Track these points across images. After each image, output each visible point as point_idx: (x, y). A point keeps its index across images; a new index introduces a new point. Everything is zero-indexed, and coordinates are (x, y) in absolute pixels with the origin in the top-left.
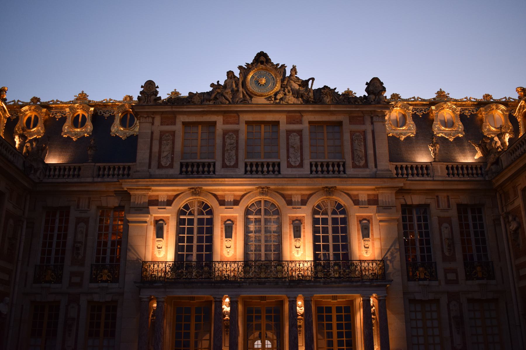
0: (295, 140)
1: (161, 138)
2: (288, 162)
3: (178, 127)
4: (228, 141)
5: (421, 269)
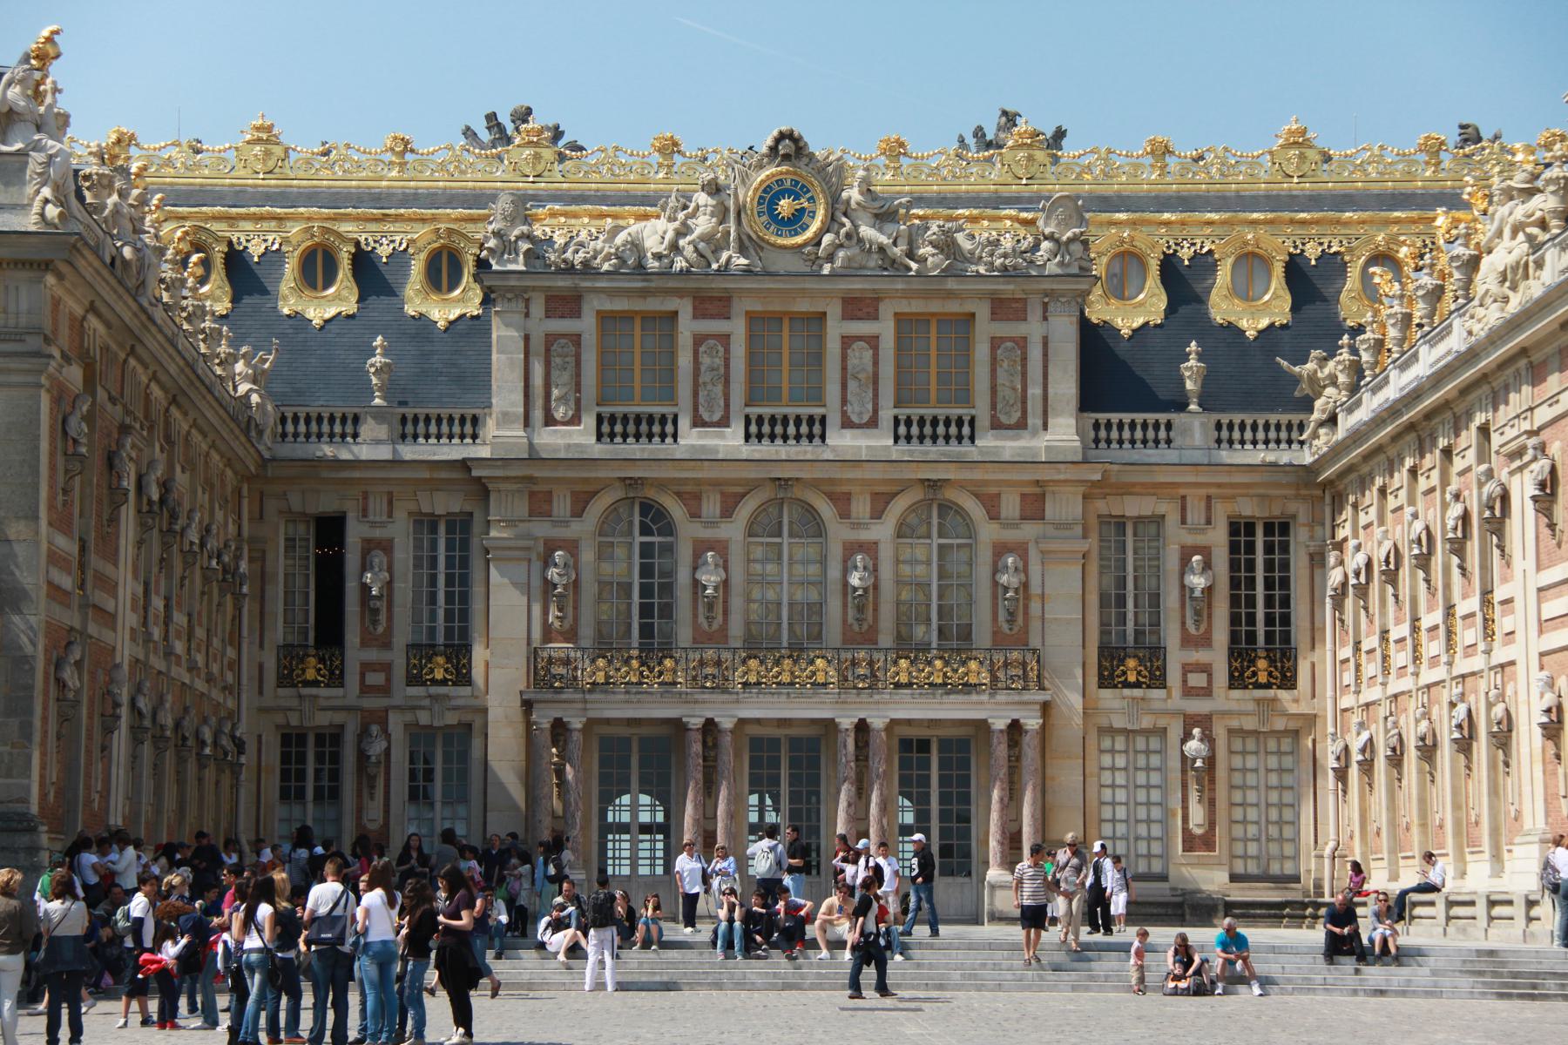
0: (861, 357)
1: (548, 350)
2: (844, 413)
3: (586, 325)
4: (706, 361)
5: (1131, 663)
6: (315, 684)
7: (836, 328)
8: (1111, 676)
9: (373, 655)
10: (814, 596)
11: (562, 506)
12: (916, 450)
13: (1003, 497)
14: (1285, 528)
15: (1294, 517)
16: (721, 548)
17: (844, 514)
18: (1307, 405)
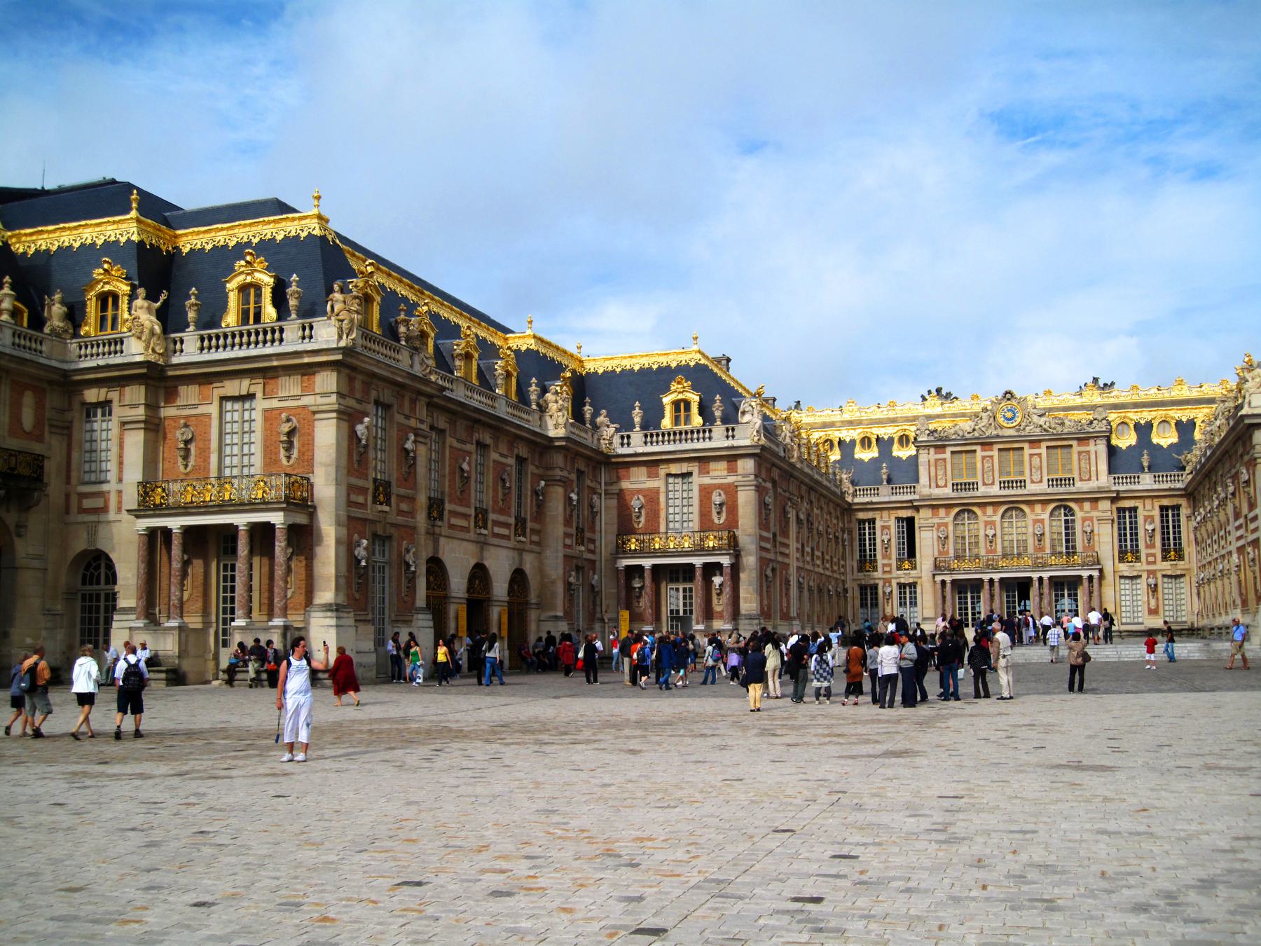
0: (1036, 461)
3: (947, 455)
7: (1028, 451)
9: (886, 561)
12: (1055, 490)
17: (1033, 510)
18: (1183, 469)
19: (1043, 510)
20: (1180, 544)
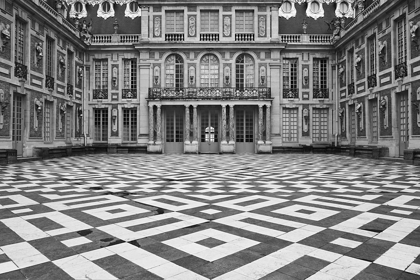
0: (227, 21)
1: (154, 20)
2: (223, 34)
3: (163, 13)
4: (191, 22)
5: (290, 92)
6: (102, 98)
7: (221, 13)
8: (286, 95)
9: (114, 91)
10: (216, 77)
11: (157, 56)
13: (261, 53)
14: (325, 62)
15: (328, 58)
16: (194, 65)
17: (224, 57)
19: (231, 57)
20: (325, 86)
